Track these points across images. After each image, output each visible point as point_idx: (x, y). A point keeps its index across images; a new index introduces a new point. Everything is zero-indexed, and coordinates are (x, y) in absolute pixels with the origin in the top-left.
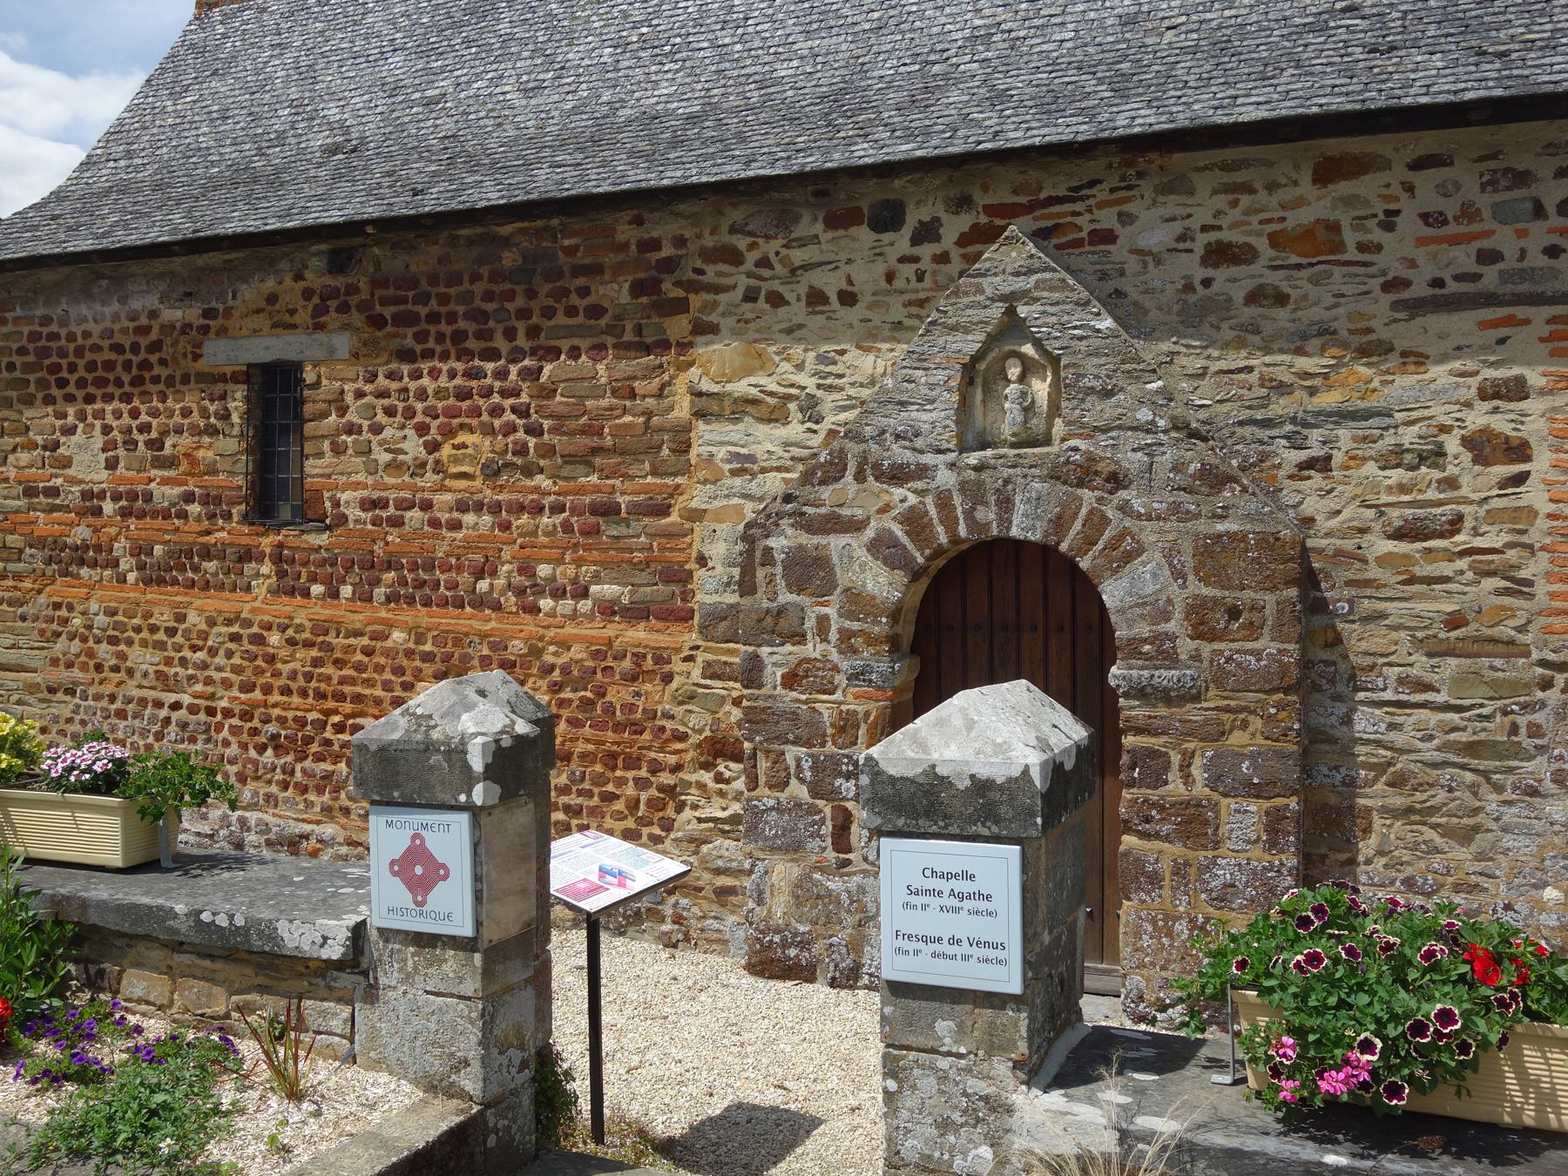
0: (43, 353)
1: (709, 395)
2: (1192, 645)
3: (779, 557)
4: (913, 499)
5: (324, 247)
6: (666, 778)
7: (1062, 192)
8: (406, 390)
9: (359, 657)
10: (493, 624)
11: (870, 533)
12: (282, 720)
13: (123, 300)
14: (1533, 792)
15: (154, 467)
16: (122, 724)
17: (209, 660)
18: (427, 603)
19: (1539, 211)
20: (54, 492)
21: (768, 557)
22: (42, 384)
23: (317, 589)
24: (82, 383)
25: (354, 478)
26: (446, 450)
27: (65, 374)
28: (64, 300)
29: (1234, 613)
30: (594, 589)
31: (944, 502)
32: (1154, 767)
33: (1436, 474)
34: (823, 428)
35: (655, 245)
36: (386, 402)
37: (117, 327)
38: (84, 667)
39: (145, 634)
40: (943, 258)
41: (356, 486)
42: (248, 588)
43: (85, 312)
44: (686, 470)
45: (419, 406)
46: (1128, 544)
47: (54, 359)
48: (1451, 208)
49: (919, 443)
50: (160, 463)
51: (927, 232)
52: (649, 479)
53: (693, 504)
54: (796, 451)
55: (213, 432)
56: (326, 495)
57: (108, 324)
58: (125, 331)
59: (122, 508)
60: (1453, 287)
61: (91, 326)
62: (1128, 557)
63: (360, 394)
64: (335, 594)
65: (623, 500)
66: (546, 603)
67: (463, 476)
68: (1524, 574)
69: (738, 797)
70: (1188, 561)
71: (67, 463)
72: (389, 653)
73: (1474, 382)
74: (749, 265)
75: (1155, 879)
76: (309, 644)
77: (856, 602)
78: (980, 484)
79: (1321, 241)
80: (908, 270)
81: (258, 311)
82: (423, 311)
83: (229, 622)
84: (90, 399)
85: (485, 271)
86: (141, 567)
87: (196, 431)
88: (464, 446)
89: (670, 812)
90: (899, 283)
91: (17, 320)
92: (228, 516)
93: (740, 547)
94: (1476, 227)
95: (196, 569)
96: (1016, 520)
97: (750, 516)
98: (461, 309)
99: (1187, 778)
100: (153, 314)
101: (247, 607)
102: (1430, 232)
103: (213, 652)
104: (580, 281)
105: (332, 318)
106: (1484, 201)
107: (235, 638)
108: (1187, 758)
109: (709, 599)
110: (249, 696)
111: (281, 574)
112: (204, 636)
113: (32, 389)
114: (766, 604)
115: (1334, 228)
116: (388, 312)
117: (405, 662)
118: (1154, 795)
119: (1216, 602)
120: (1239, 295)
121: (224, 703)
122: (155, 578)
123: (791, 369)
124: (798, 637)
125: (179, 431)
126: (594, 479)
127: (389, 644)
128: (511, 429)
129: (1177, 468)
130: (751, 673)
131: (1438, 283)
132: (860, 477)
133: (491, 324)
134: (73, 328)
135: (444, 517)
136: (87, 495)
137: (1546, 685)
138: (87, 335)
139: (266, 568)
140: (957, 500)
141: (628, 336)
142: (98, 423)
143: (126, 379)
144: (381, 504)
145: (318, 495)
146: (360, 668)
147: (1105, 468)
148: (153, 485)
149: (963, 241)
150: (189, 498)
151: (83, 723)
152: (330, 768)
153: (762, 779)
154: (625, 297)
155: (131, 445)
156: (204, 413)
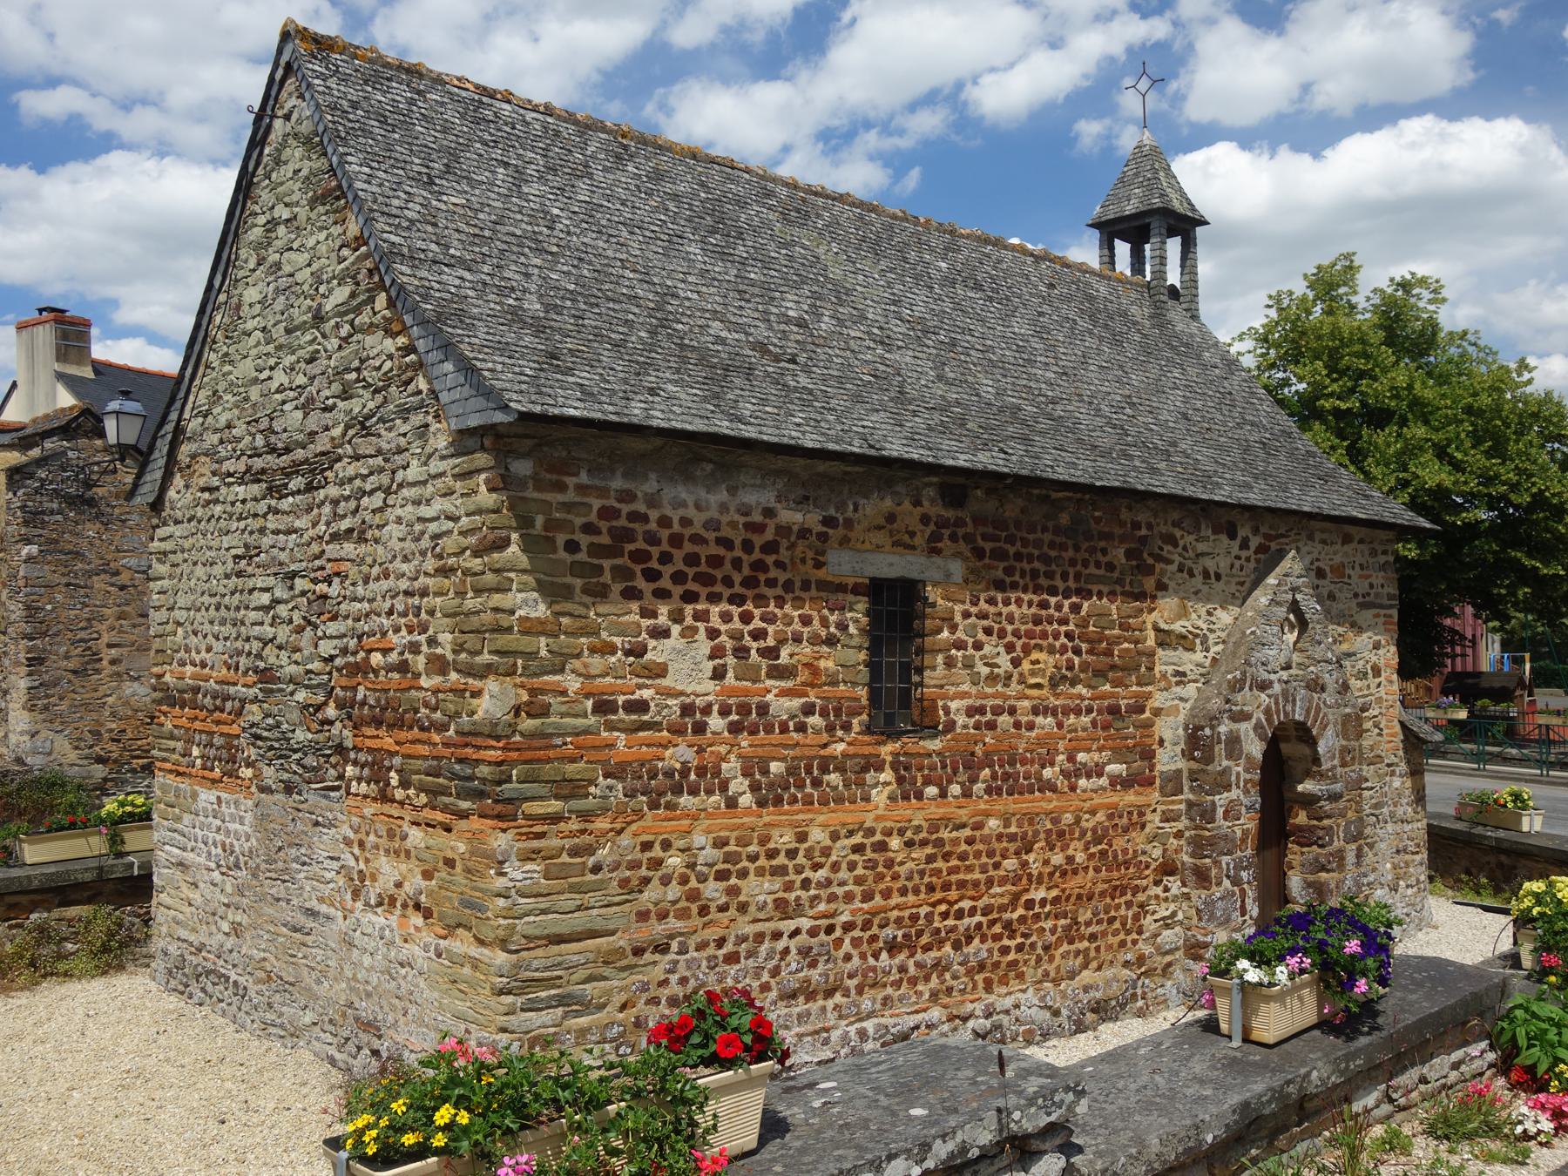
0: (626, 535)
5: (935, 480)
8: (1000, 614)
9: (964, 847)
10: (1055, 803)
13: (732, 491)
15: (769, 676)
16: (733, 970)
17: (832, 876)
20: (642, 706)
22: (622, 573)
23: (932, 791)
26: (1026, 666)
27: (654, 564)
28: (653, 476)
34: (1210, 655)
36: (985, 623)
37: (725, 519)
38: (683, 914)
39: (762, 862)
41: (963, 695)
43: (684, 495)
45: (1009, 628)
47: (640, 544)
50: (778, 672)
52: (1134, 688)
53: (1157, 705)
55: (831, 641)
56: (940, 703)
57: (713, 513)
58: (733, 525)
59: (731, 724)
61: (691, 512)
63: (966, 615)
67: (1038, 686)
71: (660, 671)
72: (986, 840)
74: (1180, 549)
76: (924, 843)
81: (880, 528)
82: (1012, 550)
84: (690, 597)
86: (755, 788)
87: (815, 640)
88: (1038, 662)
91: (581, 489)
92: (847, 727)
98: (1036, 552)
100: (769, 512)
101: (871, 816)
103: (835, 867)
104: (1102, 544)
105: (946, 544)
109: (1164, 769)
110: (871, 904)
111: (900, 780)
112: (826, 852)
113: (607, 577)
116: (988, 546)
121: (845, 918)
122: (770, 796)
123: (1196, 620)
125: (797, 639)
126: (1107, 687)
127: (986, 831)
128: (1063, 650)
133: (1054, 567)
134: (668, 512)
135: (1024, 719)
138: (686, 522)
139: (887, 775)
143: (737, 578)
144: (981, 710)
148: (769, 697)
150: (808, 710)
152: (938, 954)
155: (741, 652)
156: (825, 623)
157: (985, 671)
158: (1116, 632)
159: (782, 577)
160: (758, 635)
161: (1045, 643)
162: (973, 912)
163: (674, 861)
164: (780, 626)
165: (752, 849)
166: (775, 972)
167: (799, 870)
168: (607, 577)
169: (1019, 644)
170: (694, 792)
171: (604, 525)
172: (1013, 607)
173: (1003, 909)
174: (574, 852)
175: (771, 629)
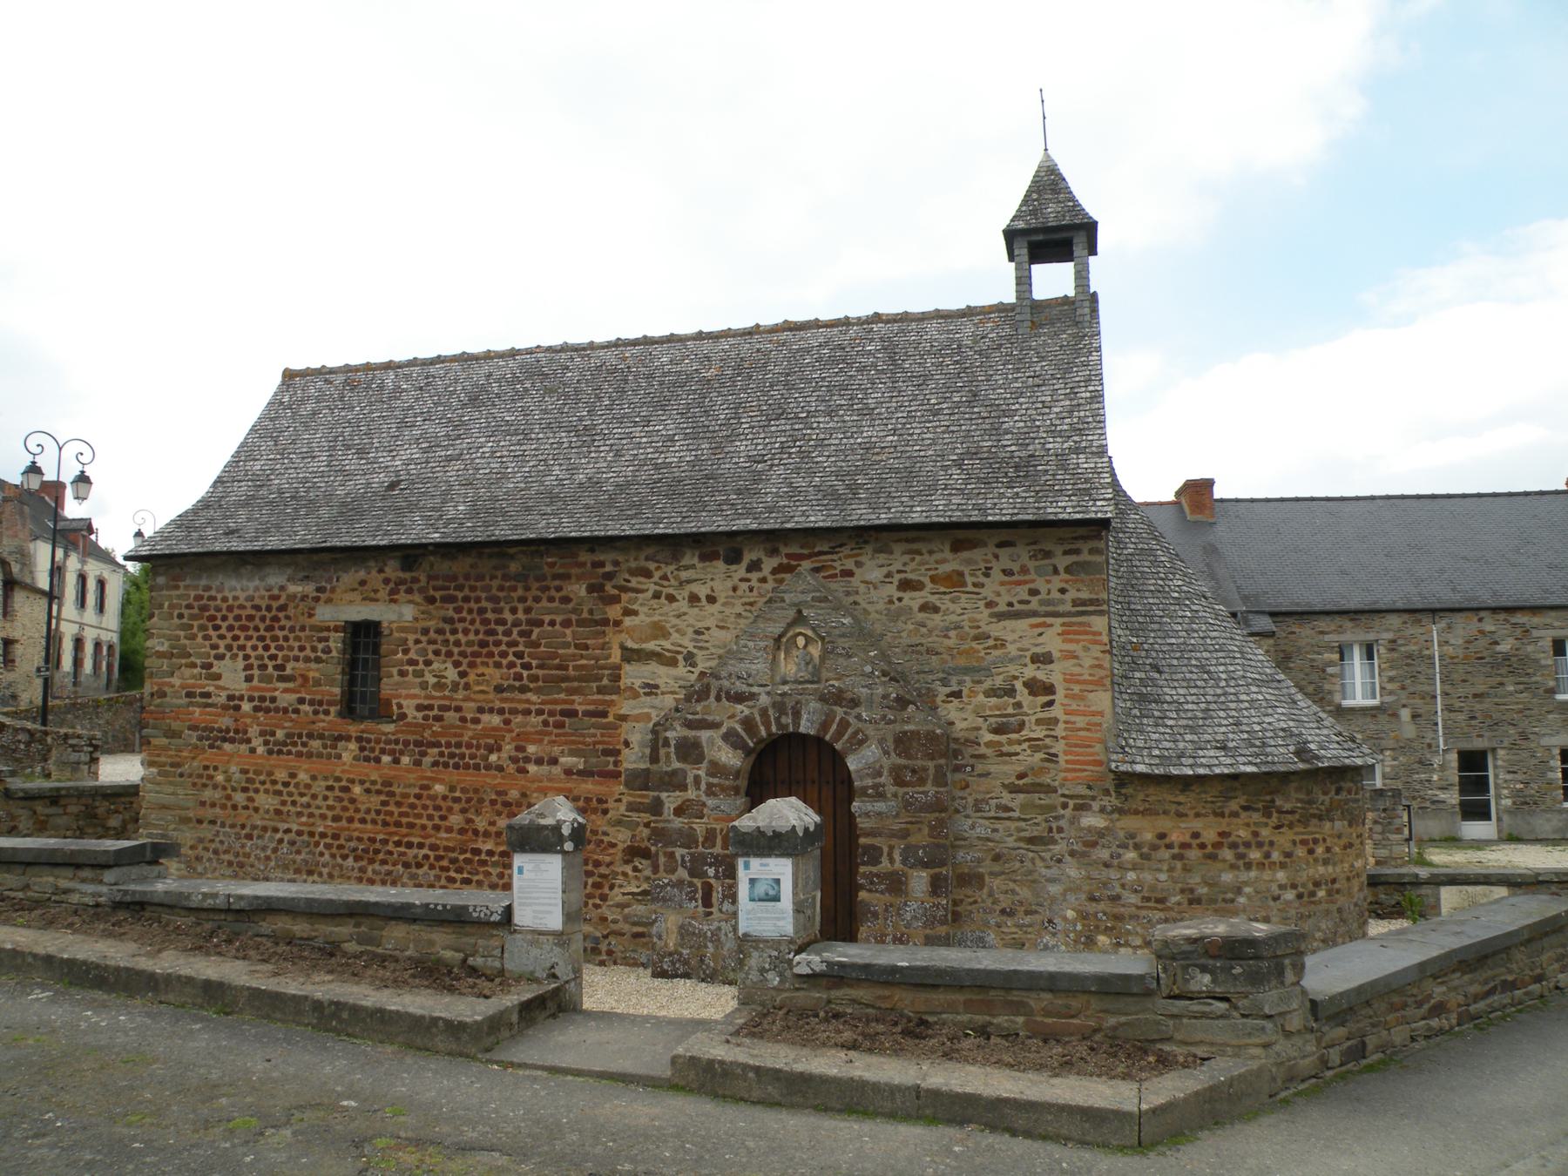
0: (204, 608)
1: (632, 650)
2: (894, 789)
3: (673, 743)
4: (747, 712)
6: (603, 870)
7: (826, 548)
11: (724, 729)
12: (360, 839)
13: (262, 579)
14: (1059, 861)
16: (249, 843)
18: (457, 766)
19: (1056, 571)
20: (207, 695)
21: (666, 743)
23: (386, 759)
24: (230, 628)
25: (413, 691)
26: (472, 678)
27: (218, 622)
29: (914, 771)
30: (562, 760)
31: (764, 712)
32: (874, 855)
33: (1012, 701)
35: (602, 564)
36: (434, 647)
38: (224, 807)
39: (268, 786)
40: (763, 580)
41: (414, 696)
42: (339, 757)
44: (617, 691)
45: (456, 650)
46: (860, 736)
47: (212, 612)
48: (1016, 567)
49: (751, 681)
50: (282, 679)
51: (754, 566)
54: (681, 683)
55: (318, 660)
58: (262, 598)
60: (1017, 607)
61: (238, 593)
62: (861, 743)
63: (417, 642)
64: (396, 761)
65: (580, 709)
66: (532, 768)
68: (1052, 751)
69: (647, 879)
70: (890, 745)
71: (218, 677)
72: (433, 798)
73: (1028, 654)
75: (875, 915)
76: (379, 792)
77: (716, 769)
78: (783, 704)
79: (955, 581)
80: (744, 586)
83: (326, 779)
85: (499, 574)
86: (266, 743)
87: (307, 660)
89: (606, 890)
90: (739, 592)
91: (186, 587)
92: (327, 713)
93: (650, 736)
94: (1027, 578)
95: (304, 745)
96: (803, 722)
97: (655, 719)
98: (484, 595)
99: (892, 861)
100: (282, 588)
102: (1007, 579)
103: (314, 797)
104: (557, 583)
105: (402, 596)
106: (1031, 564)
107: (330, 788)
108: (891, 848)
111: (362, 749)
113: (195, 630)
114: (665, 769)
115: (961, 574)
116: (438, 595)
117: (442, 804)
118: (874, 869)
119: (906, 767)
120: (915, 606)
121: (321, 829)
124: (684, 788)
125: (297, 659)
128: (511, 665)
129: (885, 697)
130: (656, 808)
131: (1010, 604)
132: (718, 699)
134: (227, 593)
135: (469, 716)
136: (231, 698)
137: (1065, 806)
138: (236, 598)
139: (353, 746)
140: (771, 712)
141: (585, 615)
142: (241, 654)
143: (262, 626)
144: (430, 707)
145: (388, 703)
146: (413, 806)
147: (849, 695)
148: (277, 693)
149: (774, 571)
150: (301, 701)
151: (222, 842)
153: (662, 868)
154: (583, 592)
155: (263, 667)
156: (314, 649)
157: (433, 680)
158: (572, 650)
159: (288, 624)
160: (273, 657)
161: (491, 661)
162: (421, 846)
163: (220, 778)
164: (285, 652)
165: (262, 778)
166: (275, 850)
167: (290, 794)
168: (195, 630)
169: (465, 661)
170: (232, 741)
171: (196, 604)
172: (460, 636)
173: (453, 850)
174: (172, 765)
175: (280, 654)
